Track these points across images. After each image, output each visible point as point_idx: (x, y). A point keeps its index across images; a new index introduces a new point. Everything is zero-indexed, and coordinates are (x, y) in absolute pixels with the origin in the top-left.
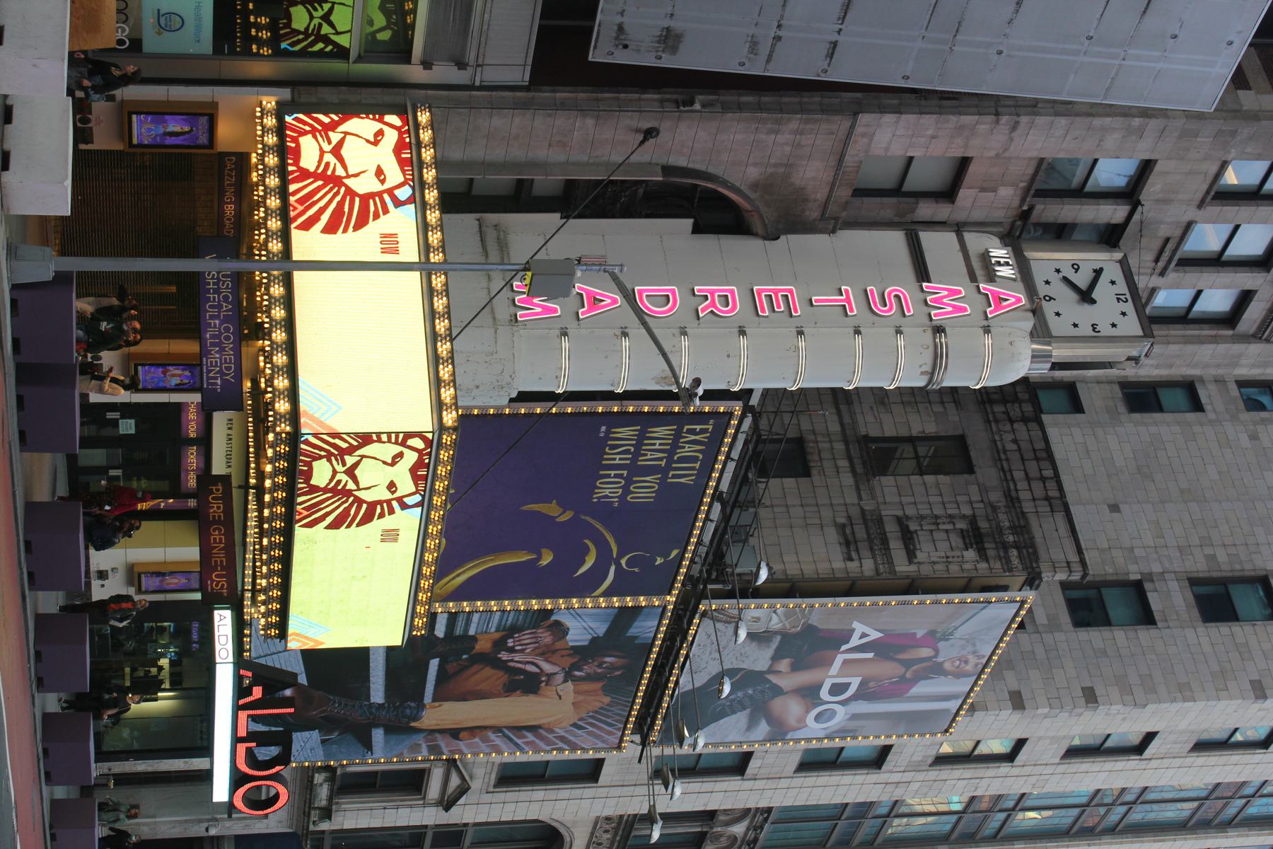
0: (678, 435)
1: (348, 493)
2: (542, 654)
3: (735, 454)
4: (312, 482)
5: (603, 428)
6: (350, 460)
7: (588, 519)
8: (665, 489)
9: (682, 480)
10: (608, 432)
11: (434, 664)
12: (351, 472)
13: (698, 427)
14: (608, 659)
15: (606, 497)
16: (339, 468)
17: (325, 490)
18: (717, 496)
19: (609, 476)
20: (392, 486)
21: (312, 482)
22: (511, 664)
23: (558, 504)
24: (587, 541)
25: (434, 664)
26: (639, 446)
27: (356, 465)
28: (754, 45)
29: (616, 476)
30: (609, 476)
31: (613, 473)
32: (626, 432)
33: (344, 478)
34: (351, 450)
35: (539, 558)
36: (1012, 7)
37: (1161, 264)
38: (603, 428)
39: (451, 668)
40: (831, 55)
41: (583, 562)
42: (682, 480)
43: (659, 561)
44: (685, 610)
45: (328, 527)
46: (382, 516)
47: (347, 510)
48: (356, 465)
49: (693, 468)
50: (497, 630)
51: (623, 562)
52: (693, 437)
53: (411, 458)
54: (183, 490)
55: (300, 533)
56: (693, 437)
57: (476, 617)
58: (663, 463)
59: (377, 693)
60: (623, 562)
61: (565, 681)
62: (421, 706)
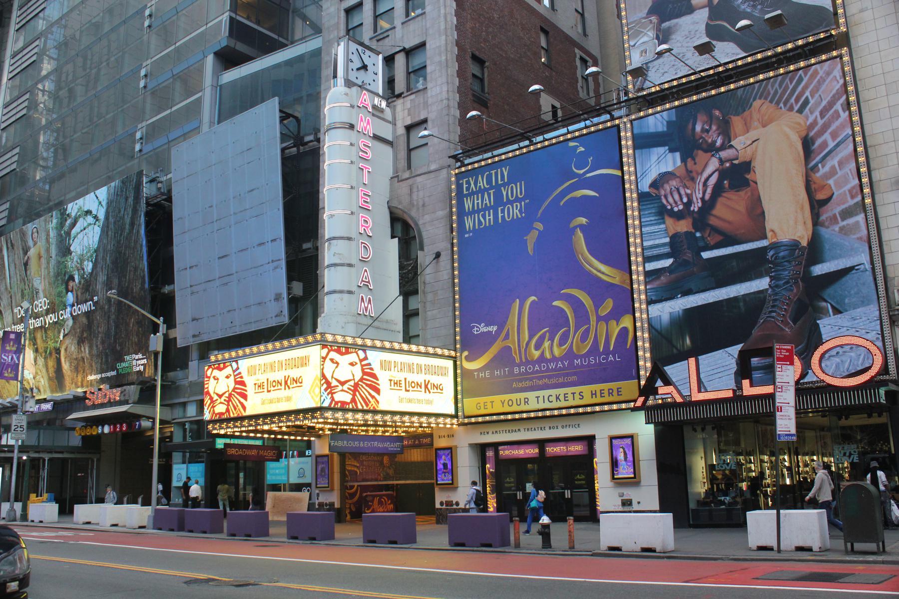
0: (473, 193)
1: (230, 395)
2: (693, 179)
3: (489, 155)
4: (224, 411)
5: (467, 236)
6: (215, 397)
7: (541, 211)
8: (512, 179)
9: (506, 174)
10: (467, 233)
11: (706, 255)
12: (220, 396)
13: (465, 186)
14: (698, 128)
15: (520, 211)
16: (218, 402)
17: (228, 405)
18: (532, 143)
19: (503, 217)
20: (227, 377)
21: (224, 411)
22: (707, 197)
23: (526, 235)
24: (562, 203)
25: (706, 255)
26: (478, 211)
27: (218, 395)
28: (276, 268)
29: (503, 211)
30: (503, 217)
31: (500, 215)
32: (469, 223)
33: (223, 398)
34: (211, 398)
35: (581, 226)
36: (254, 192)
37: (385, 35)
38: (467, 236)
39: (711, 241)
40: (275, 240)
41: (585, 197)
42: (506, 174)
43: (582, 149)
44: (673, 93)
45: (246, 399)
46: (241, 377)
47: (238, 394)
48: (218, 395)
49: (496, 174)
50: (664, 223)
51: (581, 172)
52: (472, 185)
53: (216, 373)
54: (586, 452)
55: (249, 412)
56: (472, 185)
57: (645, 244)
58: (492, 192)
59: (762, 284)
60: (581, 172)
61: (731, 147)
62: (775, 246)
